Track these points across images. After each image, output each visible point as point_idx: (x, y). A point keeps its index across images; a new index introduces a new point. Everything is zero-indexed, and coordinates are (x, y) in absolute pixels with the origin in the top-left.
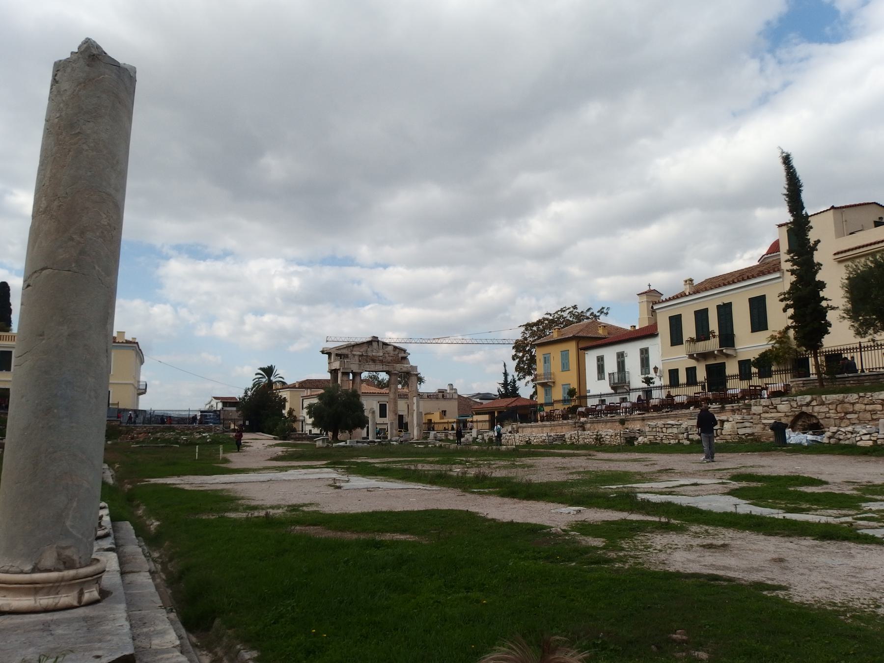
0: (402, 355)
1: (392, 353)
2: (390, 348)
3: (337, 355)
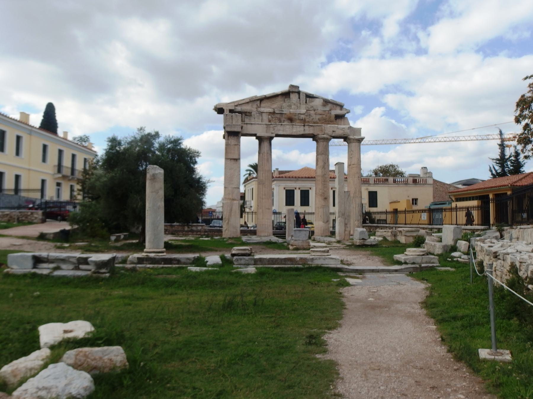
0: (338, 112)
1: (321, 109)
2: (317, 103)
3: (231, 111)
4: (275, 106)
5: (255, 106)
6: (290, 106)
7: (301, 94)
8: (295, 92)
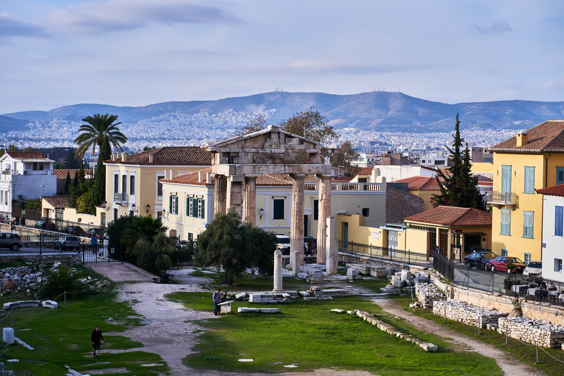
4: (256, 145)
5: (240, 146)
6: (271, 146)
7: (281, 134)
8: (275, 132)
